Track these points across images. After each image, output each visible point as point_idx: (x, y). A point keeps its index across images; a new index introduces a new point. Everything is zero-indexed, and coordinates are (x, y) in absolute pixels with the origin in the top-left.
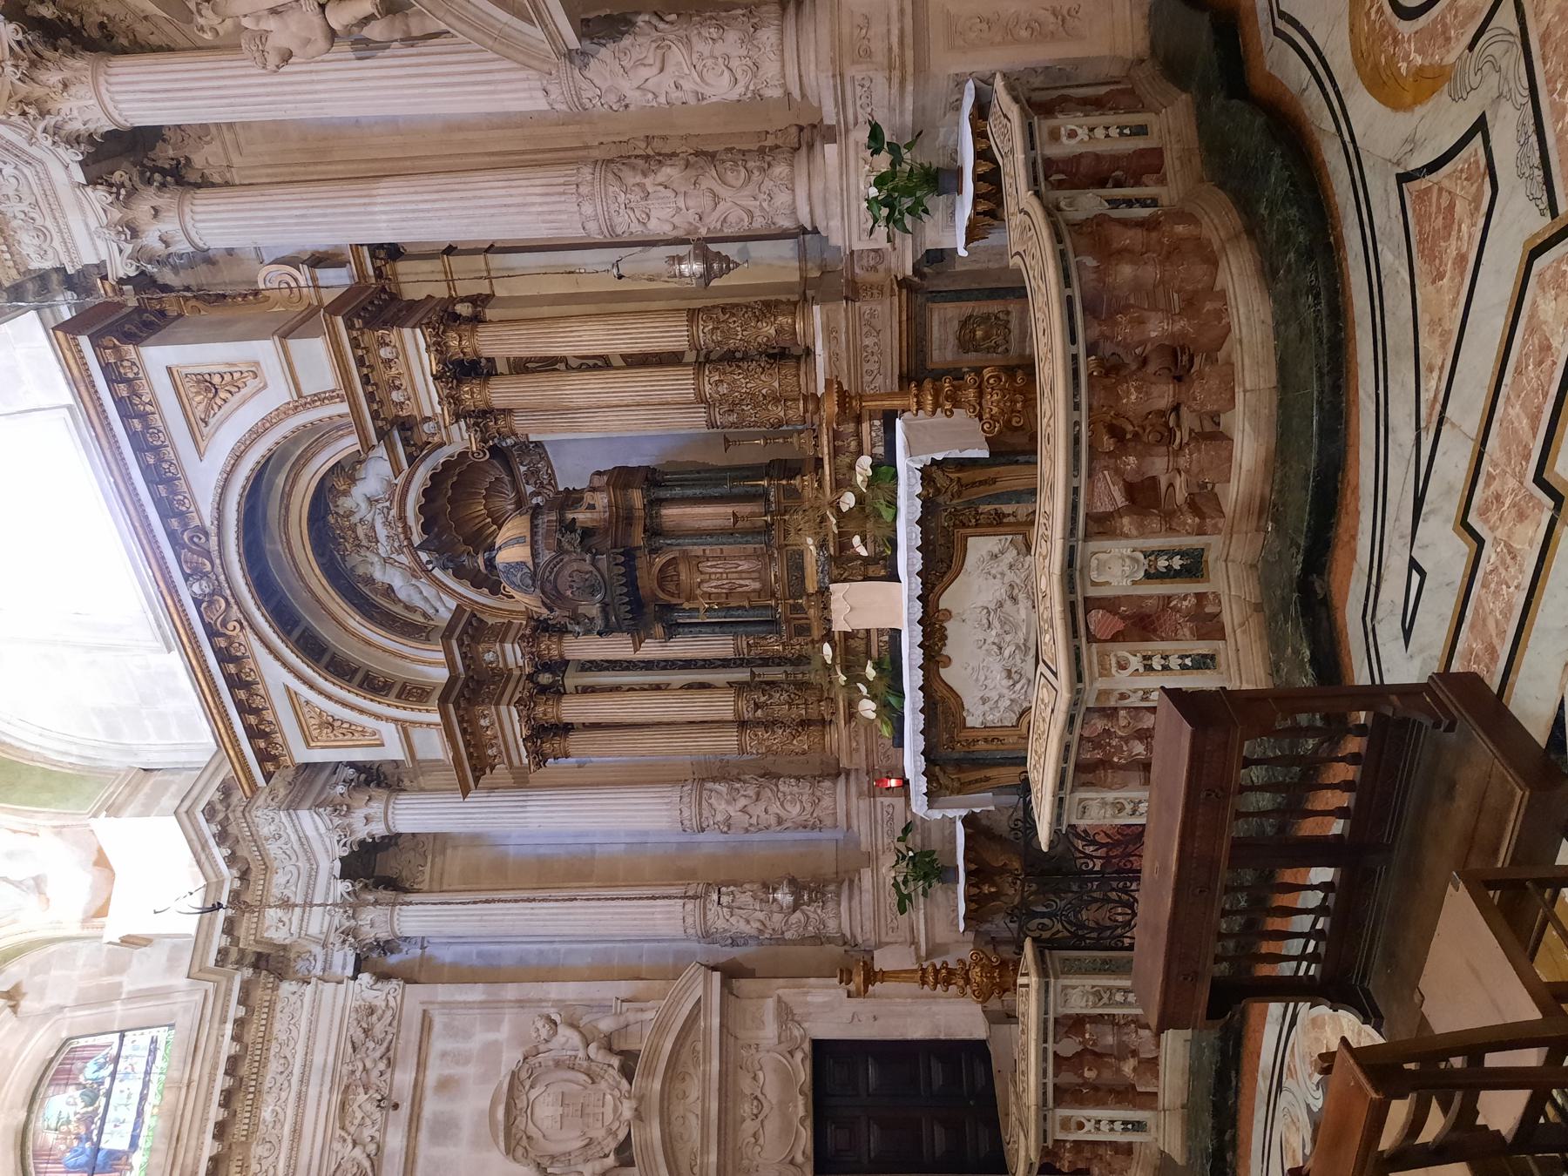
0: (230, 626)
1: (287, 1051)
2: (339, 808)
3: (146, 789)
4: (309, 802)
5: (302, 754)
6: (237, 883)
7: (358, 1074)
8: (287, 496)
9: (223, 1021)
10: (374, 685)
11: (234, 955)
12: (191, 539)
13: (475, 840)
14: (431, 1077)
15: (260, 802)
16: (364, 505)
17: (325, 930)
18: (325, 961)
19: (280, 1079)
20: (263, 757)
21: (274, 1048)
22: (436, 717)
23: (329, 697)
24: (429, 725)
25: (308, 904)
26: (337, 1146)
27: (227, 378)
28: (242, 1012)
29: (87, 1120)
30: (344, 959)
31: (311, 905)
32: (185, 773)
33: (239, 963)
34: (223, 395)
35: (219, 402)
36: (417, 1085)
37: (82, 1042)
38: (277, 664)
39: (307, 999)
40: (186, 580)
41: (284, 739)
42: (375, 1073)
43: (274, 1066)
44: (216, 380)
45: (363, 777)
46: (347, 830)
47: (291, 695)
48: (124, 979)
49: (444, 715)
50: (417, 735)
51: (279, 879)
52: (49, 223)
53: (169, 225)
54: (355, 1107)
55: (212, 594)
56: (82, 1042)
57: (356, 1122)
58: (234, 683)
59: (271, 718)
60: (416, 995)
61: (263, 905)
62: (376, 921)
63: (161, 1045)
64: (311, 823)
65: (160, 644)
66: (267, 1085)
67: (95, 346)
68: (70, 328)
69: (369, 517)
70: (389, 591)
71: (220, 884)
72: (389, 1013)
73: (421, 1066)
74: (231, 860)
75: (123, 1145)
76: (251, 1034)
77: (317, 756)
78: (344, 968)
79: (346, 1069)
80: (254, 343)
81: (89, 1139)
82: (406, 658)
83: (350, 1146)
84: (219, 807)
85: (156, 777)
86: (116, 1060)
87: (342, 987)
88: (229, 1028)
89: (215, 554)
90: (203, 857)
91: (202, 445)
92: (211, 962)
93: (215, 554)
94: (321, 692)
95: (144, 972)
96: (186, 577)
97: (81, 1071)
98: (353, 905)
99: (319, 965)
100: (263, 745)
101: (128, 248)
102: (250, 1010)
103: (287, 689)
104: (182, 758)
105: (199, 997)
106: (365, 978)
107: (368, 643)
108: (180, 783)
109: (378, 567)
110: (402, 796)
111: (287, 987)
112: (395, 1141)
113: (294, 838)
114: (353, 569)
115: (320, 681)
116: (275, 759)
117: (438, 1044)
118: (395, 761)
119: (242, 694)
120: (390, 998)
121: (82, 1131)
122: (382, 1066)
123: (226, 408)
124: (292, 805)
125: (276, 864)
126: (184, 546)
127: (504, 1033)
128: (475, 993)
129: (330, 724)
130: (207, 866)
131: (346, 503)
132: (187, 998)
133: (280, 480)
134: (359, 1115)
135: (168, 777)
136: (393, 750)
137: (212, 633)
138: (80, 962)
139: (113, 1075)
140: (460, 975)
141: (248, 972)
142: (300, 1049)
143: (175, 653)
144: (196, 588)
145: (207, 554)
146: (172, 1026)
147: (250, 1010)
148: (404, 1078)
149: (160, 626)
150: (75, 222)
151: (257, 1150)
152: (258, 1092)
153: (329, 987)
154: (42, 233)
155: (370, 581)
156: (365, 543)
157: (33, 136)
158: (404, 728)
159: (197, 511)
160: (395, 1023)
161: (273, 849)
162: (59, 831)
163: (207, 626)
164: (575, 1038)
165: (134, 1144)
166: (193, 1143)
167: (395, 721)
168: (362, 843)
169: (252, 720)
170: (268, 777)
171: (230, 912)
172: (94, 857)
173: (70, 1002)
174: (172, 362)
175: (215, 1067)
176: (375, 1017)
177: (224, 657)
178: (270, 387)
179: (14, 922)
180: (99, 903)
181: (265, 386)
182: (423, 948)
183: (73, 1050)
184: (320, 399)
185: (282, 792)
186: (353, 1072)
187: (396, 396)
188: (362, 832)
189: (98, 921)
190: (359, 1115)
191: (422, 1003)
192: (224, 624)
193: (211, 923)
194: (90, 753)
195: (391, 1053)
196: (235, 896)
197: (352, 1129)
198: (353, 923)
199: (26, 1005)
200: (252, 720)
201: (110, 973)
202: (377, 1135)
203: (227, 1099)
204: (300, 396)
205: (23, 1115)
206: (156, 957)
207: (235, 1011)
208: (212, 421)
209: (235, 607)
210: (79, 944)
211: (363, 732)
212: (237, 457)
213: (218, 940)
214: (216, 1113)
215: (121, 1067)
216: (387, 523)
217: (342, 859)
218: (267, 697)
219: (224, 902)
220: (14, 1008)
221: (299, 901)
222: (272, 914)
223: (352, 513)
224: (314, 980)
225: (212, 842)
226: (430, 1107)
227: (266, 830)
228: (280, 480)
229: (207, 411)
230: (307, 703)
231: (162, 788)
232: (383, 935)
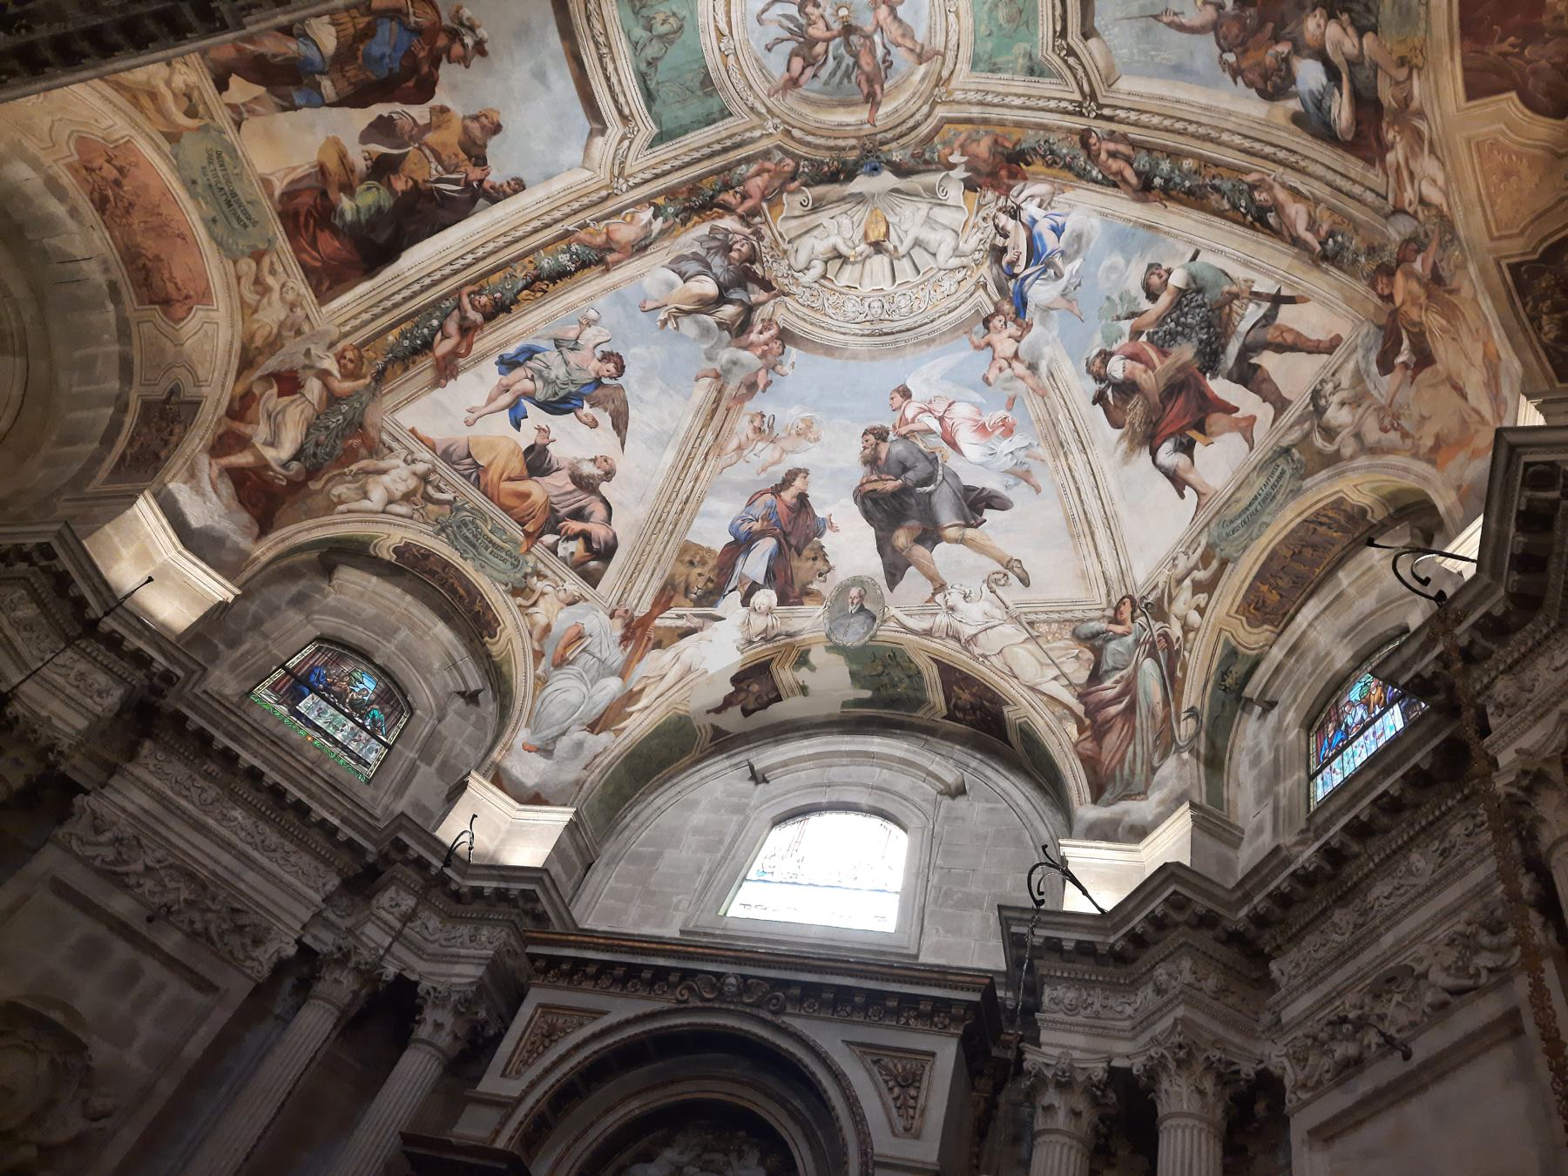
0: (685, 992)
1: (277, 855)
2: (465, 1006)
3: (575, 858)
4: (487, 980)
5: (536, 997)
6: (454, 887)
7: (209, 903)
8: (783, 1103)
9: (344, 820)
10: (566, 1096)
11: (394, 855)
12: (777, 998)
13: (347, 1124)
14: (152, 969)
15: (513, 941)
17: (364, 939)
18: (332, 924)
19: (258, 839)
20: (553, 962)
21: (289, 846)
22: (500, 1144)
23: (577, 1047)
24: (497, 1133)
25: (398, 936)
26: (160, 854)
27: (911, 1102)
28: (341, 837)
29: (341, 697)
30: (324, 941)
31: (395, 939)
32: (570, 892)
33: (384, 857)
34: (897, 1090)
35: (891, 1084)
36: (153, 949)
37: (404, 720)
38: (631, 1015)
39: (311, 893)
40: (743, 976)
41: (558, 988)
42: (197, 916)
43: (273, 839)
44: (913, 1092)
45: (480, 1041)
46: (441, 1002)
47: (597, 1014)
48: (432, 770)
49: (501, 1155)
50: (491, 1116)
51: (434, 923)
52: (1079, 1019)
53: (1061, 1120)
54: (182, 885)
55: (721, 992)
56: (404, 720)
57: (166, 880)
58: (633, 971)
59: (584, 985)
60: (238, 988)
61: (423, 898)
62: (340, 986)
63: (360, 768)
64: (466, 973)
65: (690, 927)
66: (261, 825)
67: (970, 1003)
68: (989, 992)
71: (463, 875)
72: (241, 956)
73: (169, 961)
74: (477, 893)
75: (302, 707)
76: (317, 838)
77: (526, 1010)
78: (315, 937)
79: (222, 895)
80: (937, 1145)
81: (325, 689)
82: (576, 1141)
83: (150, 863)
84: (529, 906)
85: (579, 871)
86: (373, 734)
87: (298, 927)
88: (336, 822)
89: (755, 1011)
90: (494, 872)
91: (857, 1050)
92: (402, 836)
93: (755, 1011)
94: (586, 1042)
95: (427, 783)
96: (745, 978)
97: (382, 710)
98: (369, 974)
99: (332, 917)
100: (564, 967)
101: (1049, 1073)
102: (339, 845)
103: (605, 1013)
104: (585, 896)
105: (378, 812)
106: (291, 950)
107: (607, 1112)
108: (566, 887)
110: (440, 1070)
111: (333, 882)
112: (121, 905)
113: (463, 952)
115: (596, 1046)
116: (545, 972)
117: (175, 987)
118: (479, 1079)
119: (619, 972)
120: (255, 964)
121: (335, 688)
122: (198, 926)
123: (883, 1087)
124: (493, 965)
125: (449, 926)
126: (773, 989)
127: (132, 1058)
128: (194, 1049)
129: (550, 1036)
130: (486, 872)
132: (384, 804)
133: (797, 1103)
134: (171, 885)
135: (575, 878)
136: (492, 1083)
137: (687, 974)
138: (467, 749)
139: (363, 727)
140: (225, 1043)
141: (370, 859)
142: (273, 867)
143: (677, 935)
144: (732, 980)
145: (757, 1005)
146: (368, 782)
147: (339, 845)
148: (171, 941)
149: (706, 934)
150: (1078, 1040)
151: (212, 792)
152: (262, 816)
153: (306, 915)
154: (1072, 1009)
155: (667, 1143)
156: (706, 1156)
157: (1160, 1044)
158: (507, 1106)
159: (799, 1016)
160: (228, 957)
161: (465, 931)
162: (579, 784)
163: (695, 973)
164: (60, 1135)
165: (299, 715)
166: (262, 751)
167: (520, 1100)
168: (420, 1009)
169: (591, 970)
170: (533, 958)
171: (433, 871)
172: (543, 796)
173: (440, 727)
174: (939, 1062)
175: (311, 796)
176: (248, 941)
177: (661, 974)
178: (893, 1139)
179: (527, 725)
180: (505, 782)
181: (895, 1135)
182: (278, 1017)
183: (402, 712)
185: (510, 962)
186: (214, 899)
188: (430, 1015)
189: (491, 774)
190: (171, 885)
191: (227, 991)
192: (691, 989)
193: (435, 853)
194: (627, 833)
195: (203, 940)
196: (446, 881)
197: (162, 873)
198: (351, 964)
199: (459, 703)
200: (591, 970)
201: (444, 763)
202: (139, 891)
203: (277, 792)
204: (877, 1164)
205: (378, 661)
206: (434, 802)
207: (347, 832)
208: (875, 1069)
209: (700, 1004)
210: (481, 755)
211: (525, 1063)
212: (838, 1076)
213: (416, 849)
214: (273, 777)
215: (364, 734)
217: (416, 984)
218: (605, 991)
219: (448, 871)
220: (462, 694)
221: (406, 930)
222: (408, 902)
223: (740, 1158)
224: (323, 906)
225: (503, 885)
226: (122, 951)
227: (485, 932)
228: (797, 1103)
229: (886, 1068)
230: (581, 1025)
231: (568, 868)
232: (319, 987)
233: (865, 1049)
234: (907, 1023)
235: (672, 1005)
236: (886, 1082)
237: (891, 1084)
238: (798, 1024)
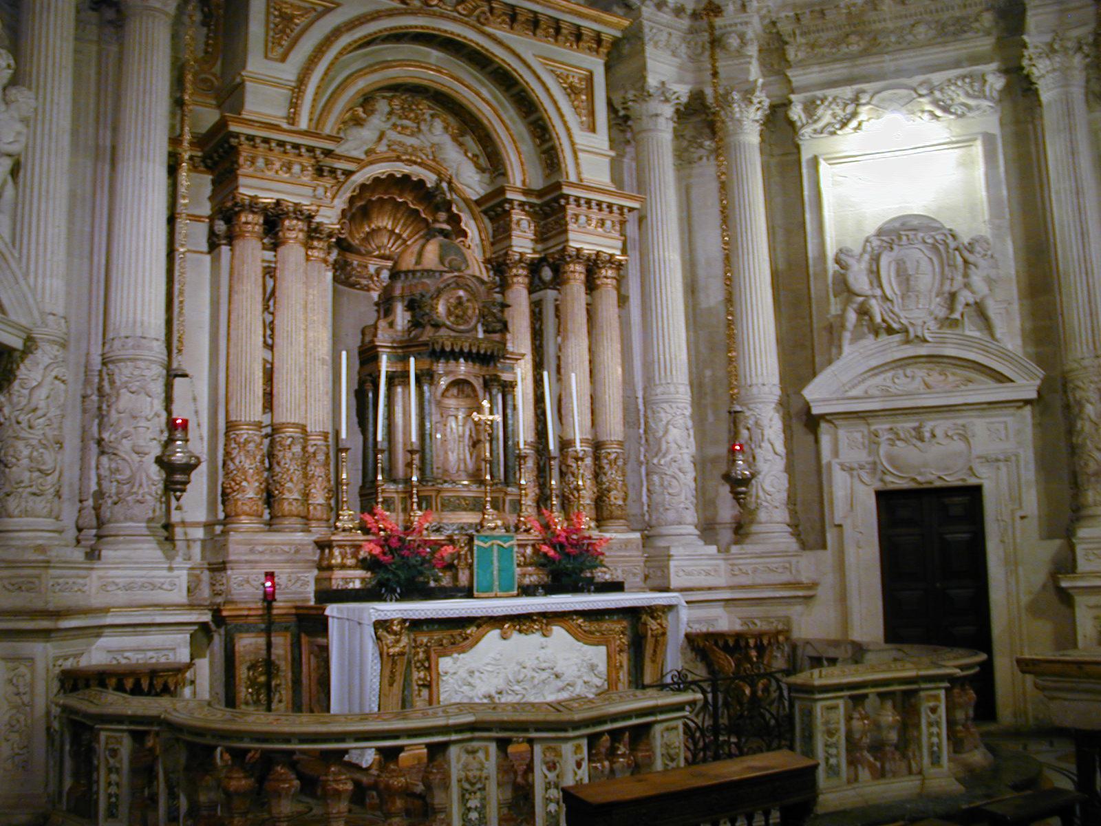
16: (436, 140)
69: (421, 136)
131: (438, 125)
234: (571, 46)
237: (569, 91)
238: (499, 33)
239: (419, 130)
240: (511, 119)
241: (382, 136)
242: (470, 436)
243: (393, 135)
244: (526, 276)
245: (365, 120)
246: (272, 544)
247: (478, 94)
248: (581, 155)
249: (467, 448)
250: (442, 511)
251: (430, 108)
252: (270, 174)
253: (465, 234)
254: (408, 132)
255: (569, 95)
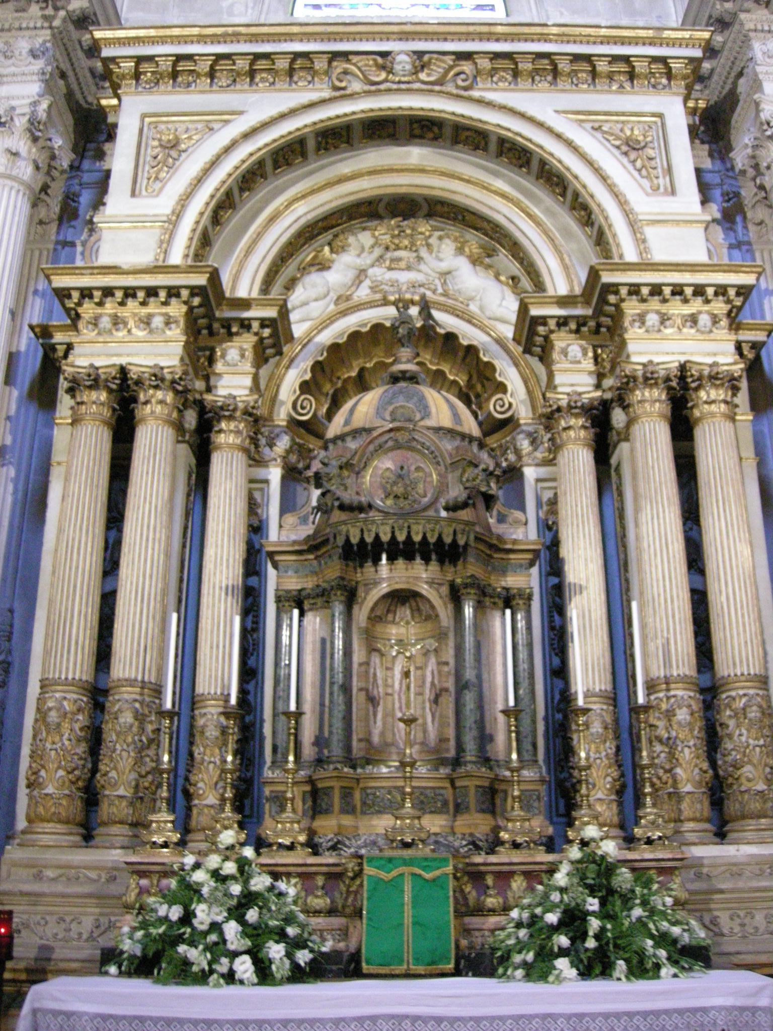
16: (444, 266)
55: (390, 71)
69: (422, 267)
70: (323, 266)
89: (437, 88)
109: (359, 261)
114: (354, 234)
131: (448, 248)
156: (389, 255)
178: (647, 199)
184: (641, 242)
187: (652, 319)
208: (599, 135)
216: (413, 286)
233: (582, 115)
234: (621, 87)
235: (326, 94)
236: (618, 147)
237: (625, 148)
239: (420, 259)
240: (548, 211)
241: (361, 274)
242: (433, 683)
243: (378, 273)
244: (584, 427)
245: (333, 261)
246: (70, 867)
247: (486, 188)
248: (650, 232)
249: (427, 705)
250: (363, 813)
251: (435, 229)
252: (121, 334)
253: (502, 388)
254: (403, 264)
255: (626, 154)
